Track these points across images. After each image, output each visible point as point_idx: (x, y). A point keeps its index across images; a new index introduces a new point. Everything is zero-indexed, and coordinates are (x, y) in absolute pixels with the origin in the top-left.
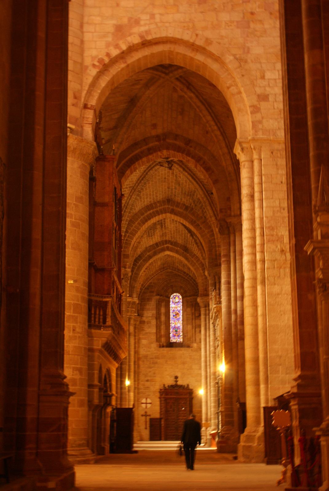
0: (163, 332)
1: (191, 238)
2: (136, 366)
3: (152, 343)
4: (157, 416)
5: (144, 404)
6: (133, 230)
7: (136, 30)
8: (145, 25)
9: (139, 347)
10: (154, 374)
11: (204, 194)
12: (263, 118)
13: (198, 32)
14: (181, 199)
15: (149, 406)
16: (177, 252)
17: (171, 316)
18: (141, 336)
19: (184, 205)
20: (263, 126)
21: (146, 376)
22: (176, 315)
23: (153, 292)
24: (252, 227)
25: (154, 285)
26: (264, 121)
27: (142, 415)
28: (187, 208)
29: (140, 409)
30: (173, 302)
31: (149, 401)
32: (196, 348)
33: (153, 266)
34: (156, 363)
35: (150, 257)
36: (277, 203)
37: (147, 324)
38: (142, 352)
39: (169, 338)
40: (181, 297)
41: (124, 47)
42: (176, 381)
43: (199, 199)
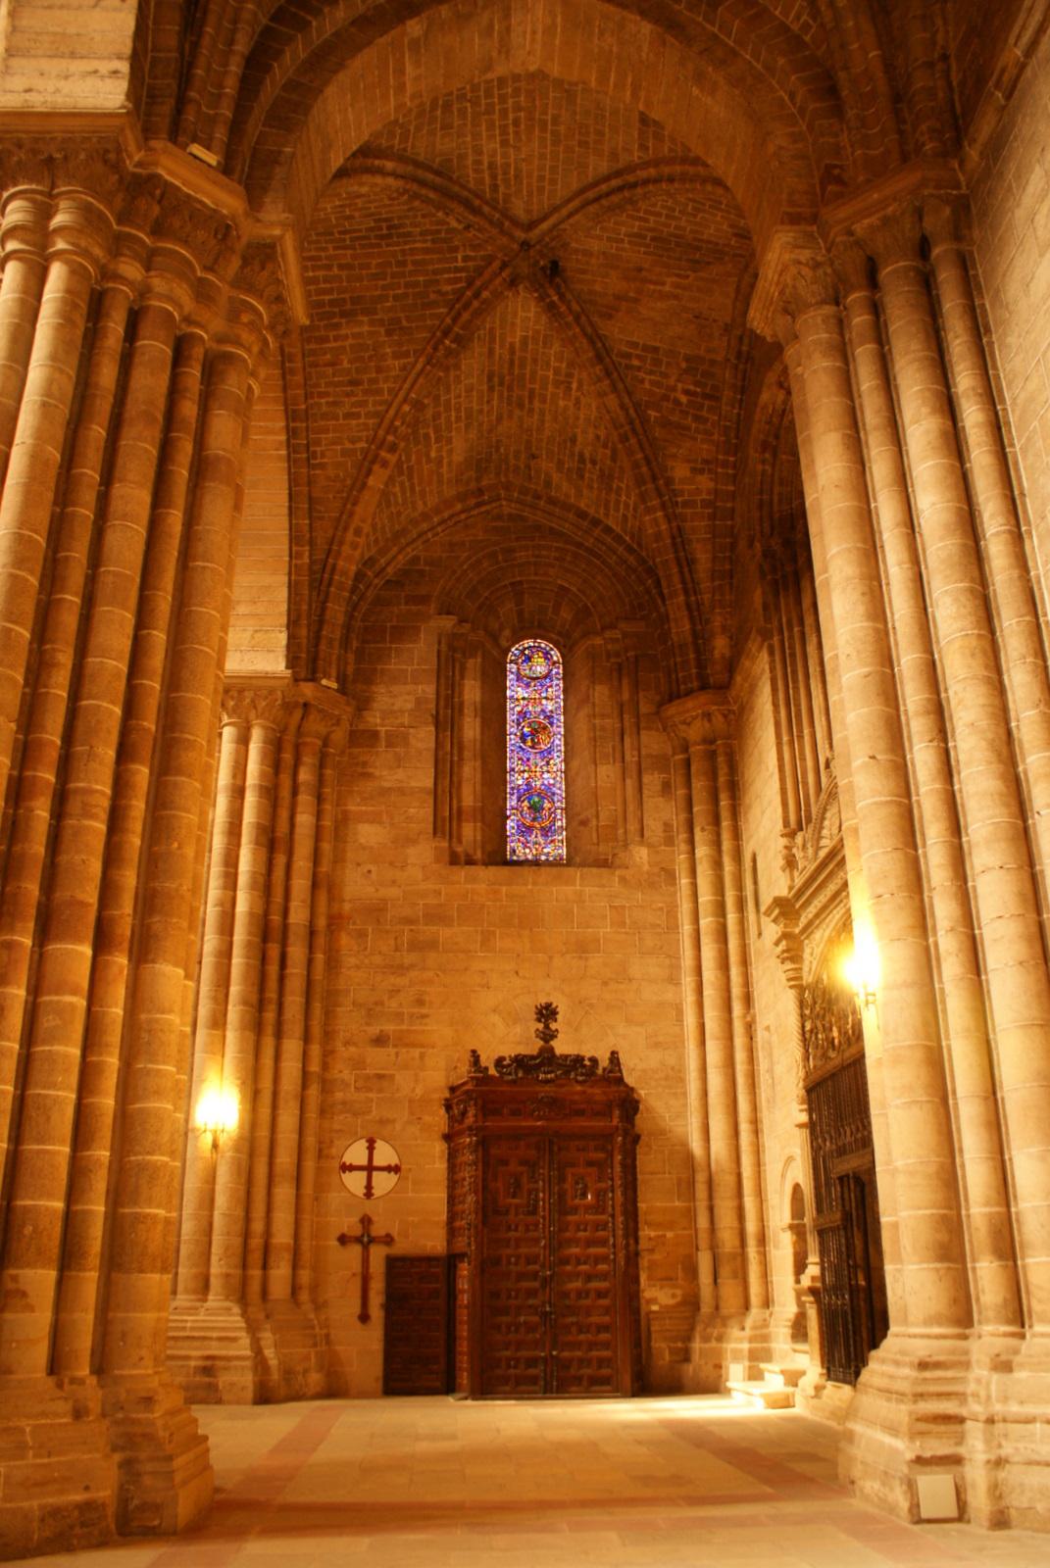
0: (469, 798)
2: (320, 957)
3: (409, 841)
4: (434, 1242)
5: (356, 1174)
9: (339, 859)
10: (420, 1002)
15: (383, 1182)
17: (512, 741)
18: (352, 808)
21: (371, 1013)
22: (534, 733)
23: (424, 600)
25: (427, 568)
27: (343, 1240)
29: (334, 1199)
30: (519, 678)
31: (384, 1154)
32: (646, 868)
33: (429, 460)
34: (432, 945)
37: (389, 745)
38: (357, 885)
39: (503, 837)
40: (556, 655)
42: (548, 1036)
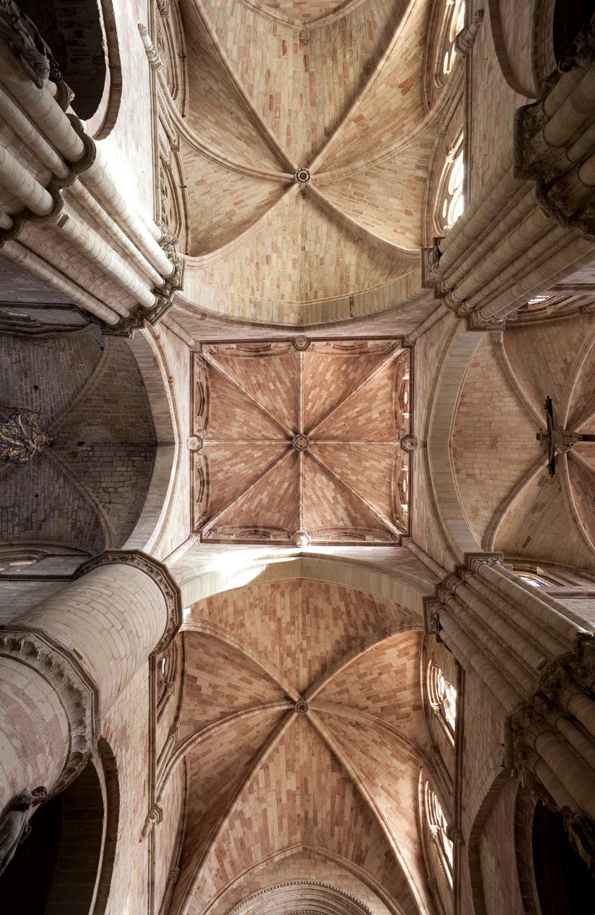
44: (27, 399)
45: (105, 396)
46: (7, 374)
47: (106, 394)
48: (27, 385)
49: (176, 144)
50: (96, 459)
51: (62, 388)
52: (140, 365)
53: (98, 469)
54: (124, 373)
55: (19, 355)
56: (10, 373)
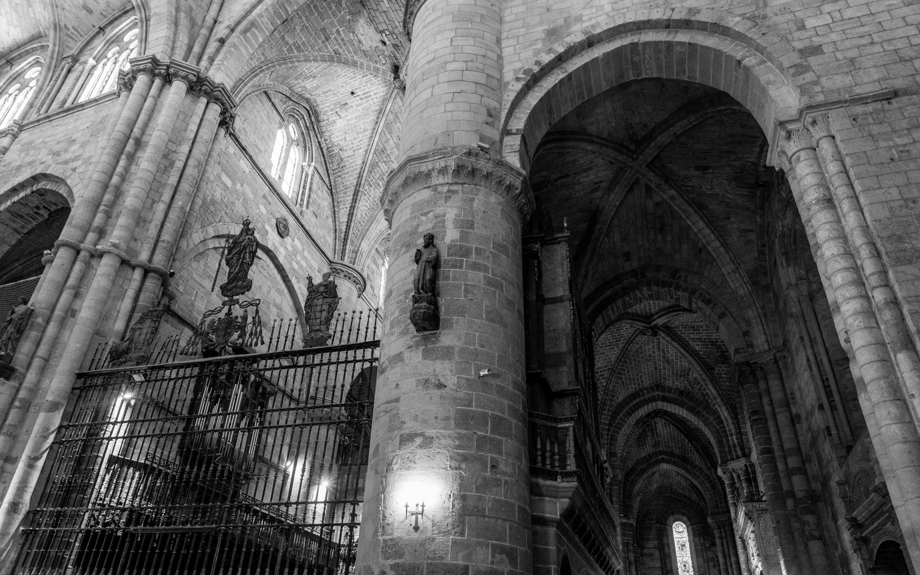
1: (690, 445)
6: (619, 423)
7: (577, 27)
8: (590, 19)
11: (702, 369)
12: (819, 77)
13: (673, 6)
14: (673, 382)
16: (675, 464)
19: (678, 389)
20: (822, 88)
24: (845, 250)
26: (823, 80)
28: (681, 393)
35: (643, 471)
36: (895, 193)
41: (561, 49)
43: (696, 379)
44: (365, 98)
45: (323, 41)
46: (351, 119)
47: (320, 42)
48: (353, 101)
49: (70, 60)
50: (390, 27)
51: (339, 76)
52: (261, 40)
53: (397, 24)
54: (287, 38)
55: (331, 114)
56: (349, 117)
